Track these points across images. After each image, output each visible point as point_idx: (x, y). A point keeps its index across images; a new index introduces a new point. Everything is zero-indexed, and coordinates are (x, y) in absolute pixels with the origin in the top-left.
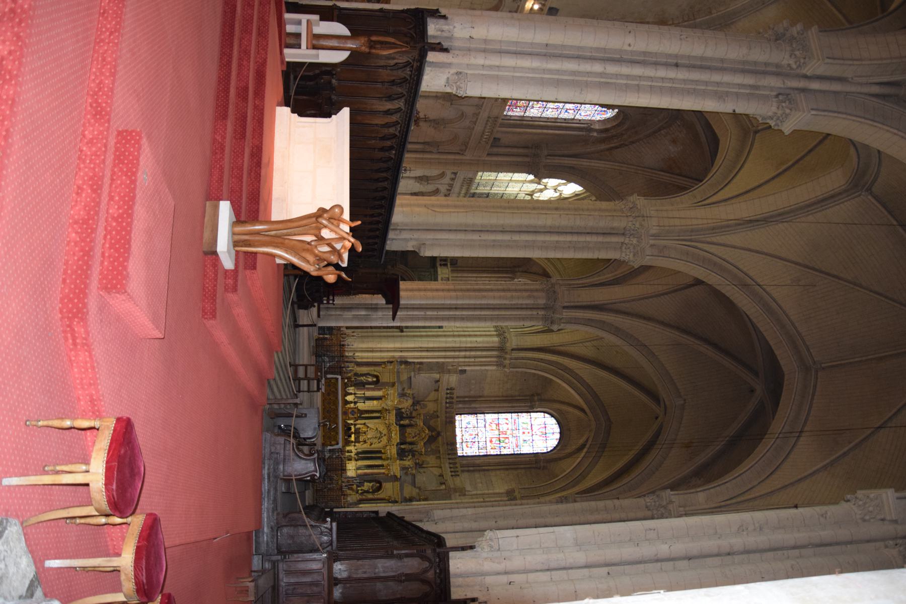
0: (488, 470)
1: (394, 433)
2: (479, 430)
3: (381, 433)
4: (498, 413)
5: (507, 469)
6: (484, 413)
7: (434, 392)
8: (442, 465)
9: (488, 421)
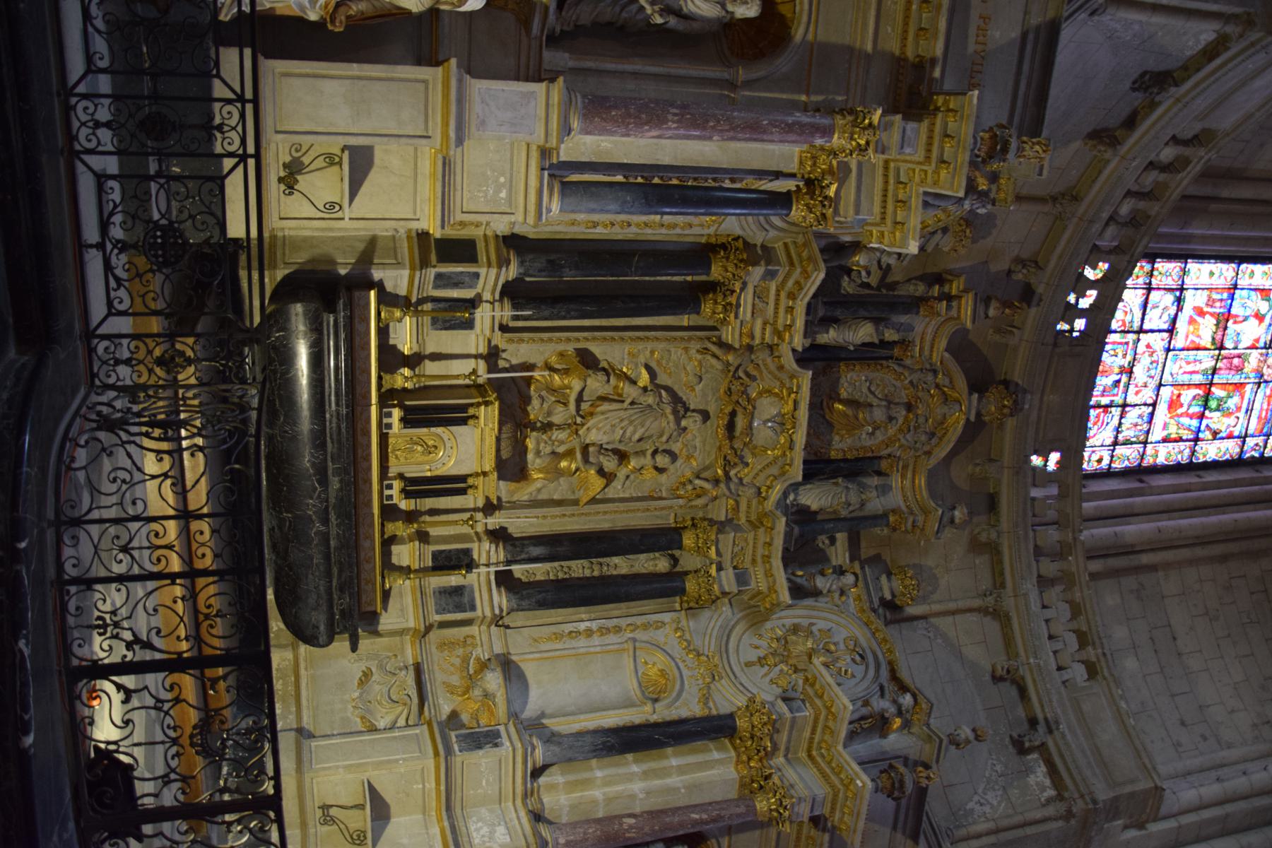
0: (1153, 568)
1: (768, 408)
2: (1141, 347)
3: (680, 406)
4: (1241, 259)
5: (1224, 558)
6: (1183, 257)
7: (1077, 144)
8: (1009, 603)
9: (1193, 300)
